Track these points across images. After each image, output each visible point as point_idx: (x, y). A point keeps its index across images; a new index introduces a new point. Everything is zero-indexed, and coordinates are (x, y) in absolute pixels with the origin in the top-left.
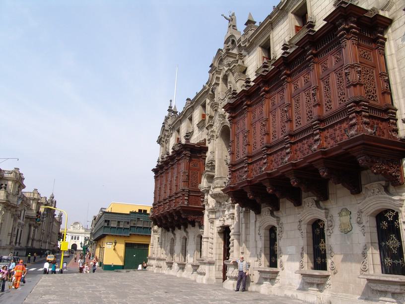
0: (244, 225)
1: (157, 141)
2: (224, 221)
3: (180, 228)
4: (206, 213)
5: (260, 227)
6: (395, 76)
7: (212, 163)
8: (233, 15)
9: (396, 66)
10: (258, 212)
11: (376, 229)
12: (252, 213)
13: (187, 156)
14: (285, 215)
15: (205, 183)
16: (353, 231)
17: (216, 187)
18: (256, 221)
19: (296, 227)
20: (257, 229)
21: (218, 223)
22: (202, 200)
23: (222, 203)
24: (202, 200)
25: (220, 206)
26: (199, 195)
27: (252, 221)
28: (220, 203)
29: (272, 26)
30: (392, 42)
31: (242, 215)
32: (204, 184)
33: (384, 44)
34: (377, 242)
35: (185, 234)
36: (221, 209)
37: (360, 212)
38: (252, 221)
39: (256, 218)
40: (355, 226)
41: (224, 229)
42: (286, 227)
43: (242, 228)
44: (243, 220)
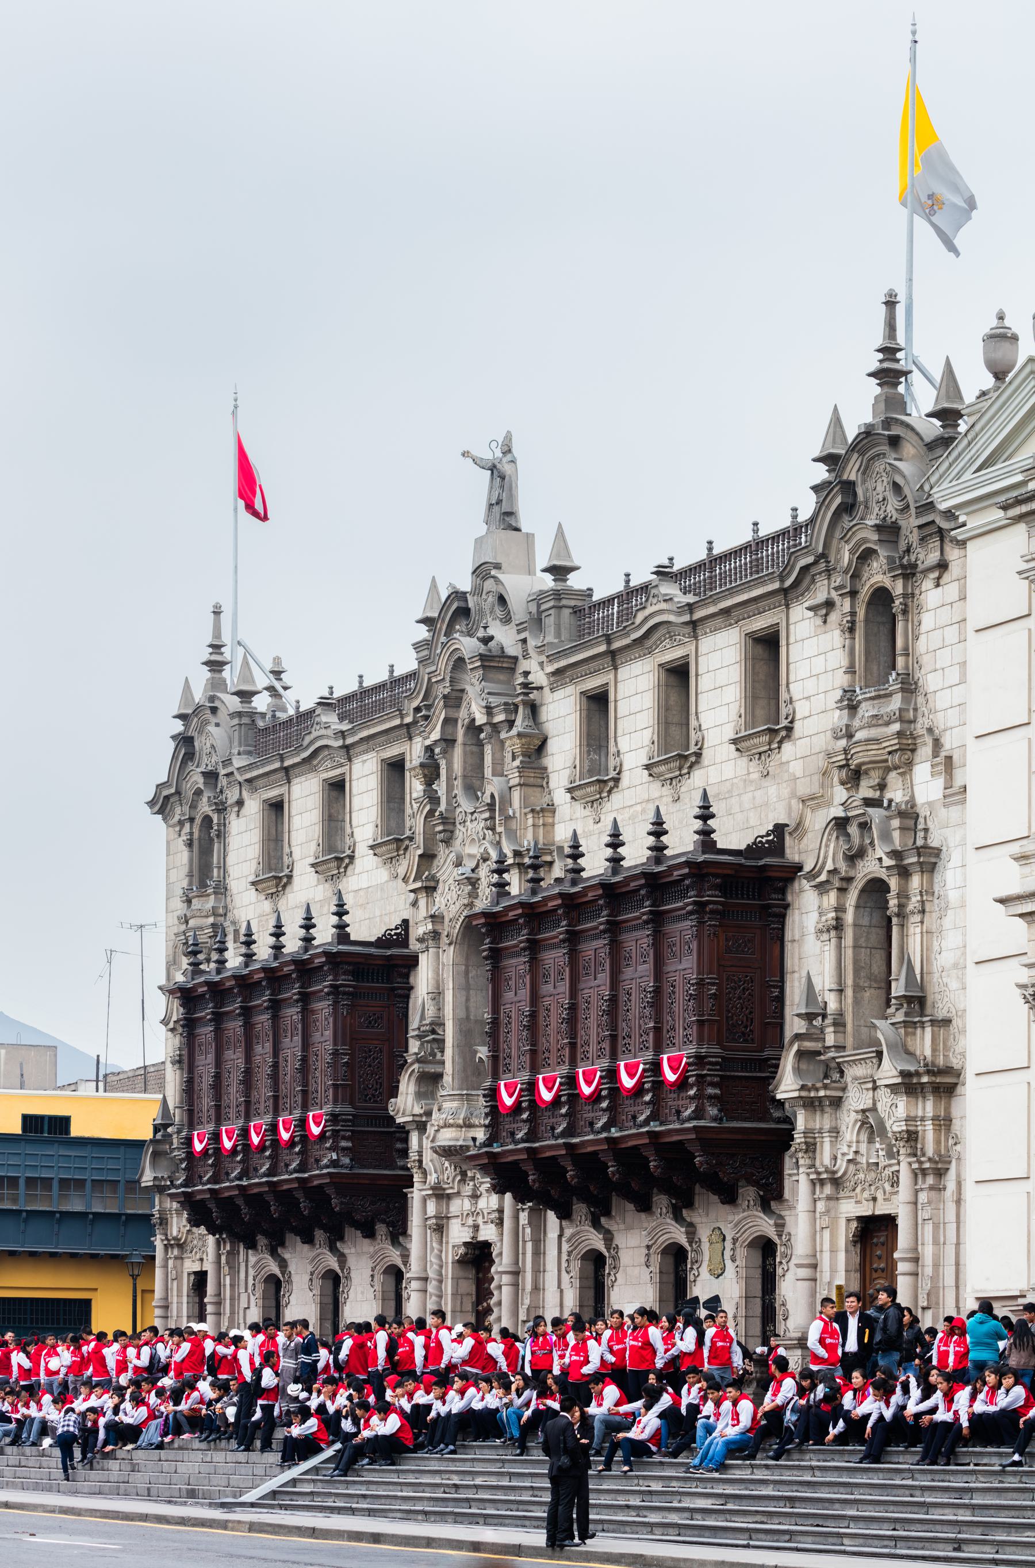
0: (529, 1246)
1: (151, 804)
2: (476, 1228)
3: (308, 1240)
4: (416, 1194)
5: (569, 1253)
6: (793, 992)
7: (433, 1032)
8: (508, 437)
9: (796, 969)
10: (565, 1214)
11: (759, 1271)
12: (551, 1216)
13: (345, 993)
14: (622, 1226)
15: (410, 1098)
16: (725, 1274)
17: (451, 1126)
18: (560, 1236)
19: (643, 1260)
20: (564, 1257)
21: (458, 1234)
22: (399, 1146)
23: (470, 1174)
24: (399, 1146)
25: (463, 1181)
26: (389, 1141)
27: (552, 1234)
28: (464, 1174)
29: (613, 660)
30: (797, 911)
31: (524, 1217)
32: (405, 1103)
33: (783, 916)
34: (759, 1294)
35: (333, 1263)
36: (467, 1190)
37: (735, 1241)
38: (552, 1234)
39: (562, 1229)
40: (728, 1263)
41: (477, 1252)
42: (626, 1257)
43: (524, 1254)
44: (528, 1230)
